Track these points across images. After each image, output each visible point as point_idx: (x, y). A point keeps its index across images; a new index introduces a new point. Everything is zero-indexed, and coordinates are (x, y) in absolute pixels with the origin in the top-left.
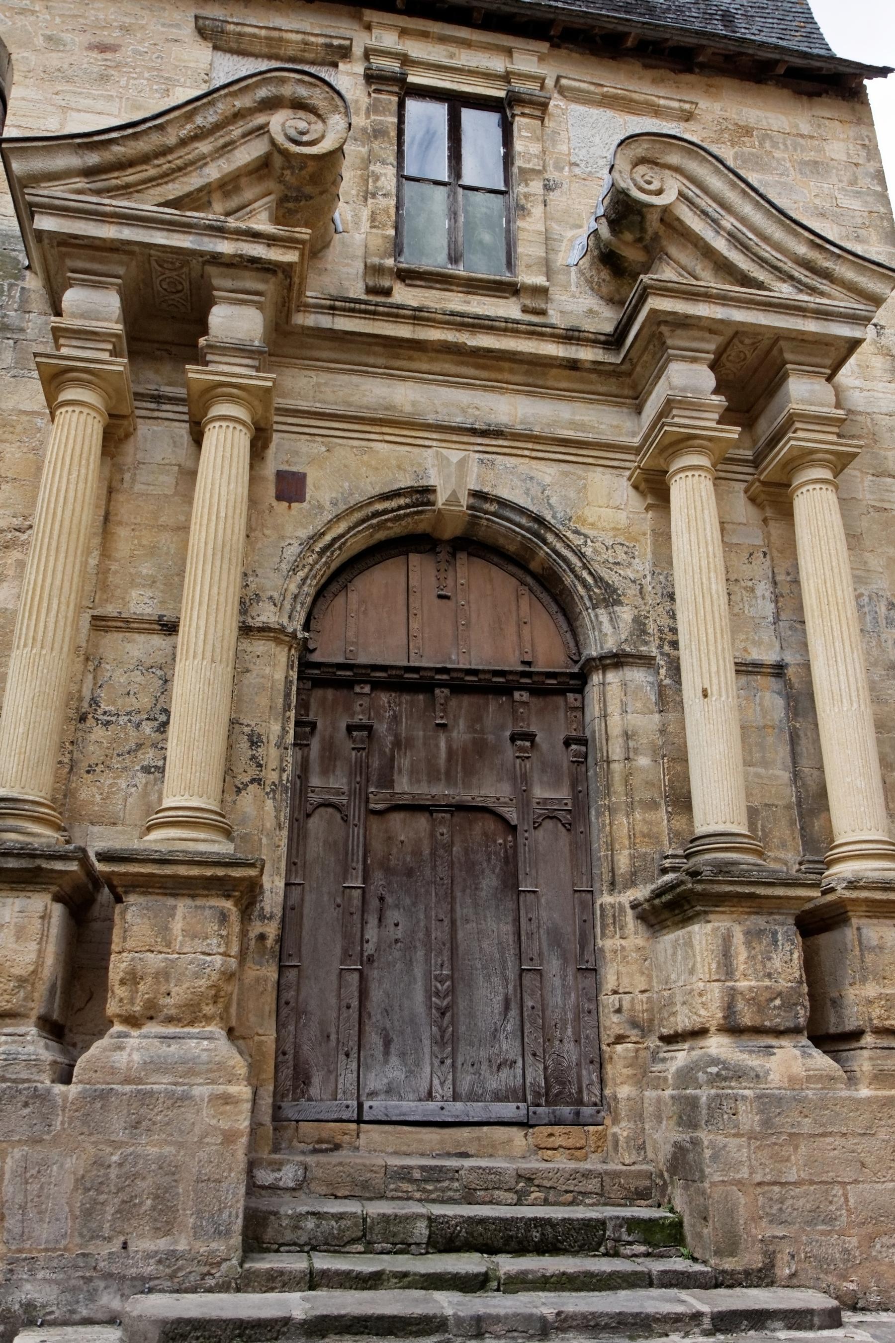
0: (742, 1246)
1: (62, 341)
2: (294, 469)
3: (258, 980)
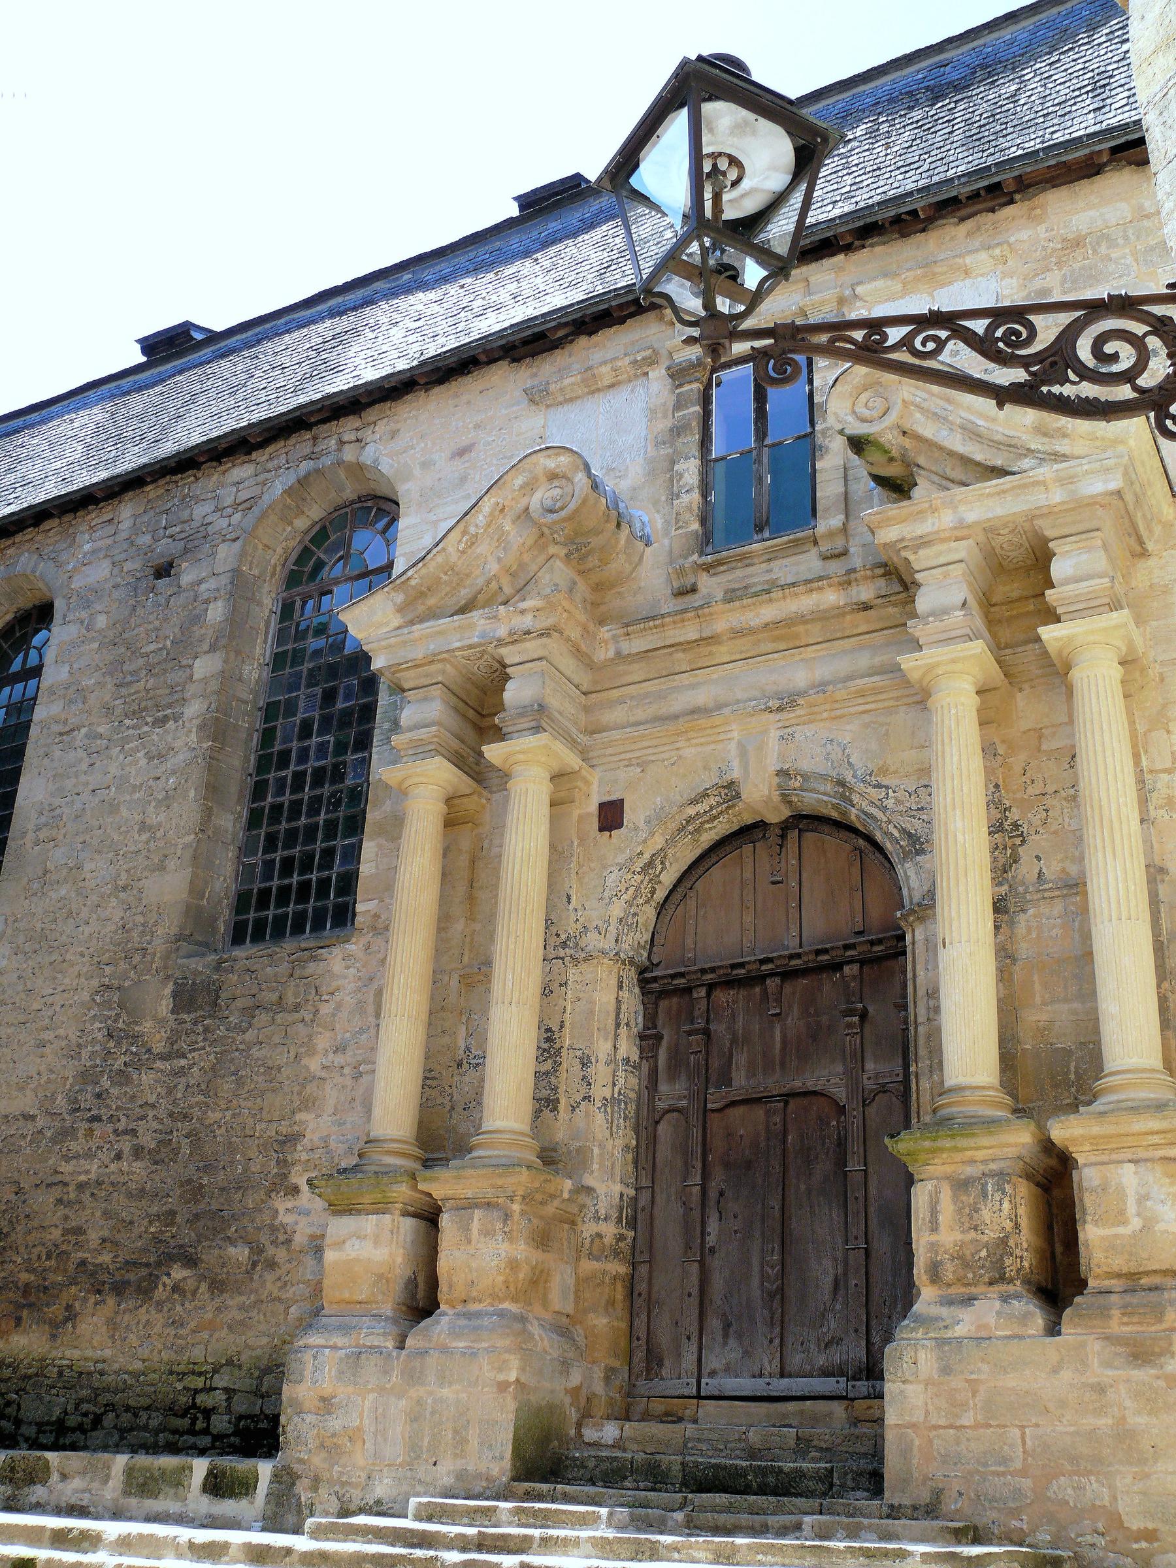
2: (614, 798)
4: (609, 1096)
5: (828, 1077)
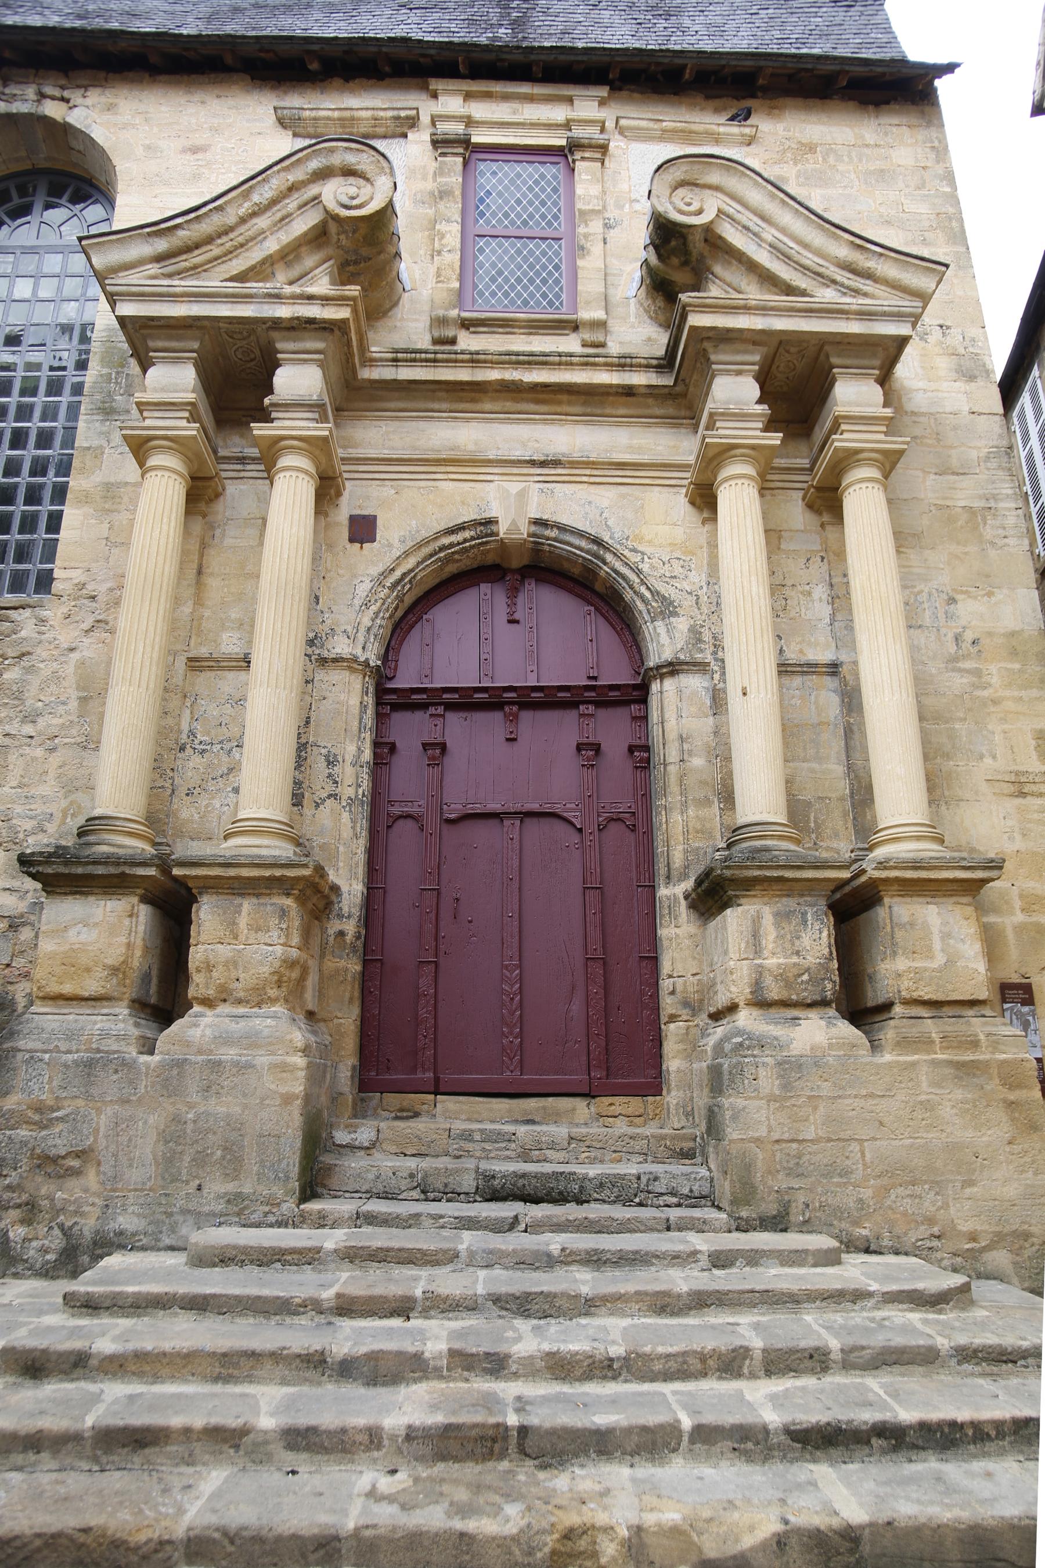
0: (758, 1196)
1: (145, 414)
3: (337, 971)
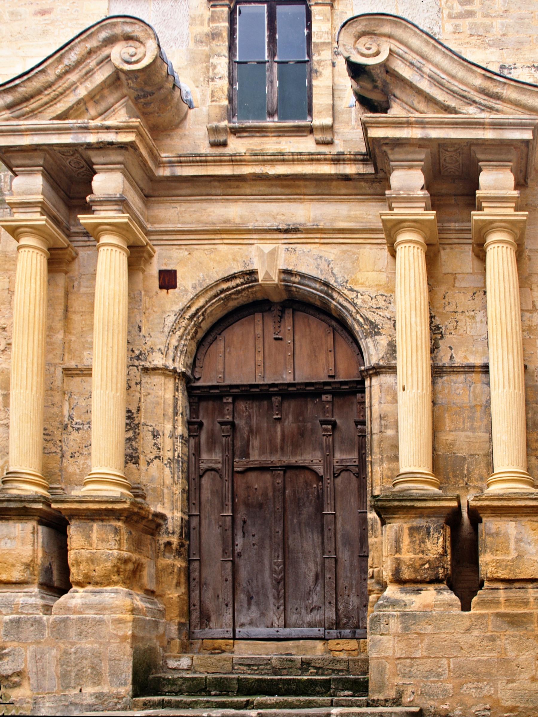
4: (172, 458)
5: (311, 457)
